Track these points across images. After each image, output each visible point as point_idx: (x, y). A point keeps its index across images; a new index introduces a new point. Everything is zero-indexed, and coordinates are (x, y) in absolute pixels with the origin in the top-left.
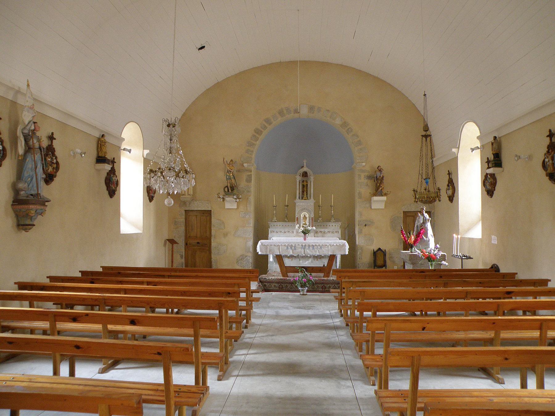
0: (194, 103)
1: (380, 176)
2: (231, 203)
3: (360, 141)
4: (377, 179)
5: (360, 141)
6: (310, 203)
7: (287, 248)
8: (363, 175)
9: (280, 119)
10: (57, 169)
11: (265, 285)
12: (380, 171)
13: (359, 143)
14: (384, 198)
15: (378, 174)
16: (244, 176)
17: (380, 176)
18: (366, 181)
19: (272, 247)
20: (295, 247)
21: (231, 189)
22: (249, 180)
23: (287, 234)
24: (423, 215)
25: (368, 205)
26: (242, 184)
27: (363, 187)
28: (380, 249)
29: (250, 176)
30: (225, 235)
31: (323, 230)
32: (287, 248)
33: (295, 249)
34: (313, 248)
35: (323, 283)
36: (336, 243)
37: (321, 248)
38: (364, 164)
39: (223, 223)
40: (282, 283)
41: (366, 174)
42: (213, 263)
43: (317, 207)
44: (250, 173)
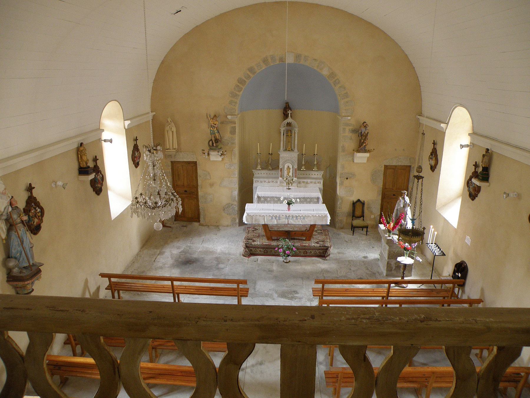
0: (173, 49)
1: (365, 132)
2: (215, 157)
3: (347, 93)
5: (347, 93)
6: (294, 155)
7: (272, 218)
8: (348, 129)
11: (251, 250)
12: (365, 127)
13: (346, 95)
14: (367, 155)
15: (363, 130)
16: (229, 128)
17: (365, 132)
18: (351, 134)
20: (279, 217)
21: (215, 143)
22: (233, 132)
23: (271, 184)
24: (404, 198)
25: (350, 159)
26: (227, 136)
27: (347, 141)
28: (359, 200)
29: (234, 128)
30: (212, 185)
31: (305, 180)
32: (272, 218)
33: (279, 219)
34: (297, 219)
36: (318, 214)
37: (304, 218)
38: (349, 118)
39: (209, 173)
40: (267, 248)
41: (351, 128)
42: (200, 211)
44: (233, 125)
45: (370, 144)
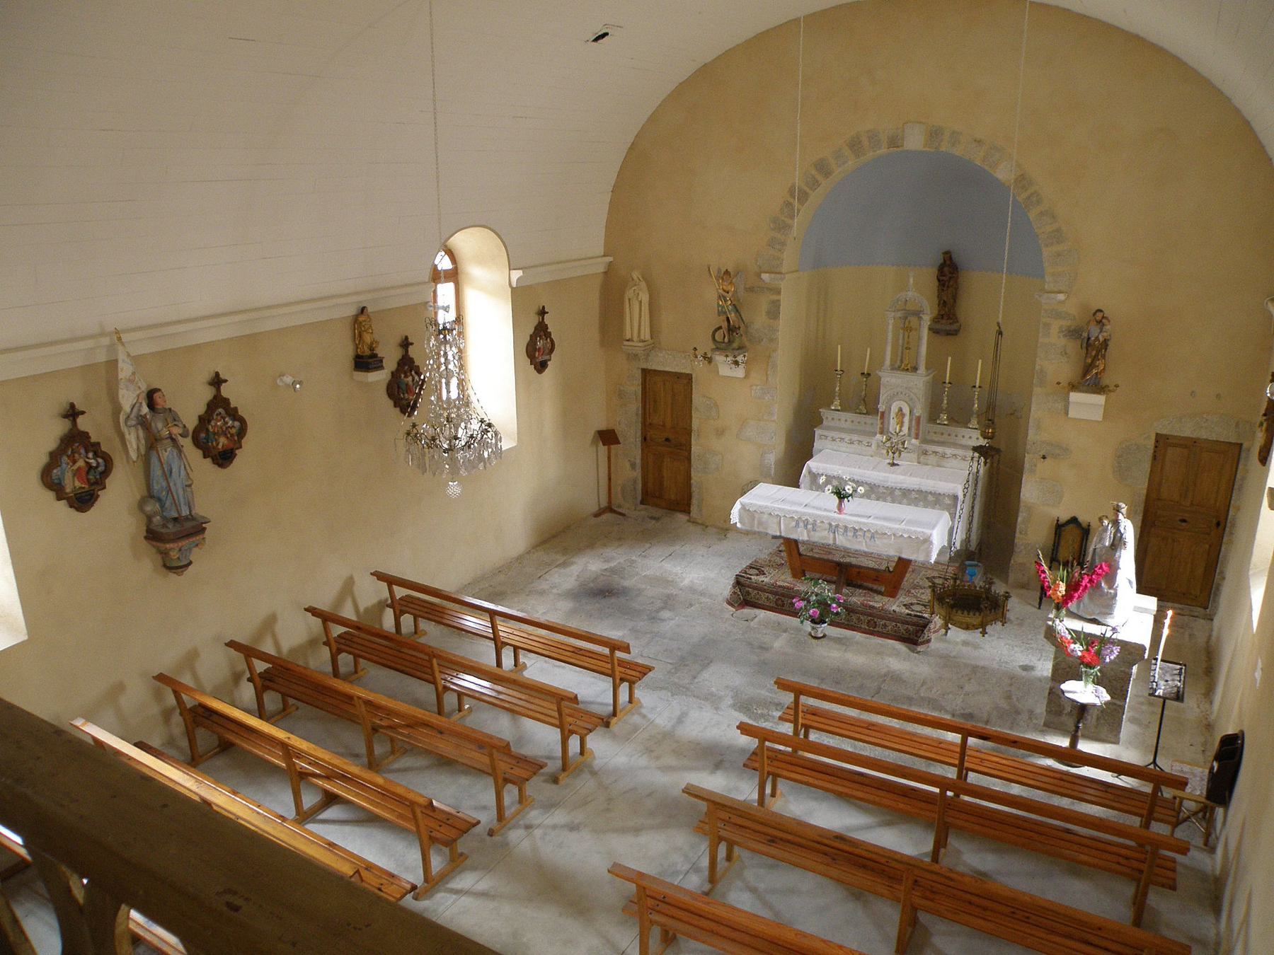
0: (652, 119)
1: (1097, 338)
2: (723, 365)
3: (1058, 230)
4: (1088, 345)
5: (1058, 230)
6: (918, 383)
7: (797, 524)
8: (1056, 325)
9: (852, 163)
10: (242, 432)
11: (748, 593)
12: (1100, 322)
13: (1057, 236)
14: (1100, 399)
15: (1094, 330)
16: (764, 302)
17: (1097, 338)
18: (1063, 341)
19: (766, 516)
20: (814, 524)
21: (732, 336)
22: (774, 313)
23: (856, 446)
24: (1116, 523)
25: (1060, 406)
26: (758, 321)
27: (1055, 358)
28: (1074, 520)
29: (776, 305)
30: (720, 433)
31: (940, 449)
32: (797, 524)
33: (814, 530)
34: (855, 535)
35: (871, 615)
36: (908, 531)
37: (873, 537)
38: (1061, 297)
39: (716, 405)
40: (783, 595)
41: (1066, 323)
42: (693, 489)
43: (936, 387)
44: (775, 297)
45: (1115, 370)
